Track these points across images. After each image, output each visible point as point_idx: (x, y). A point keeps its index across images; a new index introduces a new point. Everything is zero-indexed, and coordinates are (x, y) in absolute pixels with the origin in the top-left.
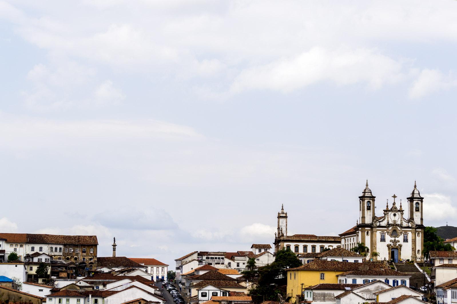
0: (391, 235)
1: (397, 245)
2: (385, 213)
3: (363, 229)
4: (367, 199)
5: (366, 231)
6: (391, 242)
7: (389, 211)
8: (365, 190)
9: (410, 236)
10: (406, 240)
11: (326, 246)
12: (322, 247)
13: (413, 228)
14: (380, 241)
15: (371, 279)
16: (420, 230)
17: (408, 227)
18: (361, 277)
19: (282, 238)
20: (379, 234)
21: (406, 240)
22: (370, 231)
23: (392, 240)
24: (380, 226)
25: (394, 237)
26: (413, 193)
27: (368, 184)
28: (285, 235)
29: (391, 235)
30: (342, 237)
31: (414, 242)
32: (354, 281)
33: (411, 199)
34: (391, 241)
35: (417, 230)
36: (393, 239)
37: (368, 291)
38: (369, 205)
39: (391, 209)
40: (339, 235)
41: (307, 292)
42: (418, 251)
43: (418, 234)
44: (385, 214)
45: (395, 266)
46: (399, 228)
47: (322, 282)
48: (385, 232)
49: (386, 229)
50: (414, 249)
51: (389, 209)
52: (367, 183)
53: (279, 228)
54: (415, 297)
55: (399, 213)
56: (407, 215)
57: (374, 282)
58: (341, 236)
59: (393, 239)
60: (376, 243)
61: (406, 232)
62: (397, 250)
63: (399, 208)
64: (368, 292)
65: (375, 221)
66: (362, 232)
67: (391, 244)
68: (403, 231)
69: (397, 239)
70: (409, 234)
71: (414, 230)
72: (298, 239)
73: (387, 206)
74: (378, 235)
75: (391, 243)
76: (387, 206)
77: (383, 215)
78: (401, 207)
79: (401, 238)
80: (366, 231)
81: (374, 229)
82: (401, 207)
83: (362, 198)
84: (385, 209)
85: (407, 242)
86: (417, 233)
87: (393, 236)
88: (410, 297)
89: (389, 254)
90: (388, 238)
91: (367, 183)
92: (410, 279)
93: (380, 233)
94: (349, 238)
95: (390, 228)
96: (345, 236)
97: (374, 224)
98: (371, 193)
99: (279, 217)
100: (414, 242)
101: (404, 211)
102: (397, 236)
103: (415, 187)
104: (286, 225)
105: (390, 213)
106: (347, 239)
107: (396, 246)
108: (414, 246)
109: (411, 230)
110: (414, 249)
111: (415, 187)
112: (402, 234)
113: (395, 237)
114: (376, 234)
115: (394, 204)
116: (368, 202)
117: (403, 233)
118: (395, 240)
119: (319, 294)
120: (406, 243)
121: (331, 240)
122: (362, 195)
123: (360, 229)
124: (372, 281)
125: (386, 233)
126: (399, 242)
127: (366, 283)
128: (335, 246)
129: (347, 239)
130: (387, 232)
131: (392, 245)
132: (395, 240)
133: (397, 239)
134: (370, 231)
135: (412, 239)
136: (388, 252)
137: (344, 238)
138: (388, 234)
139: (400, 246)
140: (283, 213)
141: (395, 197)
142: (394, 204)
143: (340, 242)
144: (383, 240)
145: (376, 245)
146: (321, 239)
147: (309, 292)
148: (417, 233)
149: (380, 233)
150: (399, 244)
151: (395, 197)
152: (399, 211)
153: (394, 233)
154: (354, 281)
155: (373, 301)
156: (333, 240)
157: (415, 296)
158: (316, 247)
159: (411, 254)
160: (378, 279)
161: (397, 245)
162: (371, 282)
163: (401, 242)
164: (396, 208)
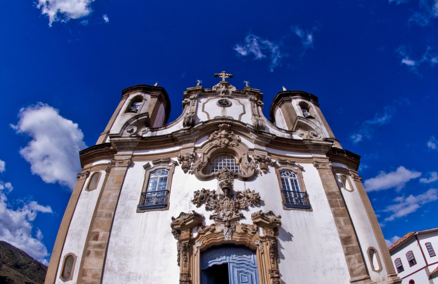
0: (204, 172)
1: (242, 221)
6: (204, 206)
14: (135, 209)
23: (204, 191)
25: (218, 176)
29: (206, 172)
36: (213, 185)
46: (248, 142)
59: (213, 185)
75: (201, 210)
87: (217, 173)
107: (239, 229)
110: (355, 244)
117: (274, 165)
120: (302, 214)
130: (182, 159)
131: (208, 222)
132: (228, 190)
133: (238, 186)
149: (147, 167)
159: (348, 273)
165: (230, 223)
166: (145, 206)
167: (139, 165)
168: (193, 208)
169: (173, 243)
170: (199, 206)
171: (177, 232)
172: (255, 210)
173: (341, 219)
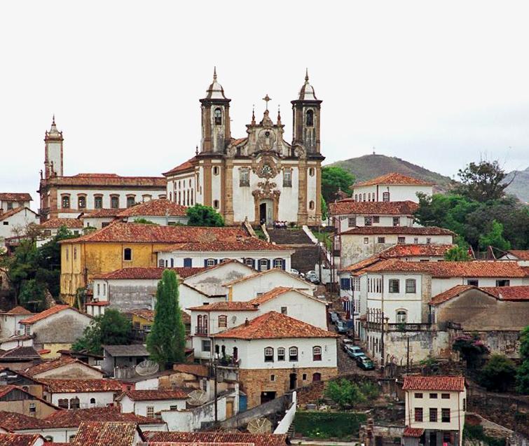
2: (249, 131)
3: (208, 161)
4: (215, 106)
5: (213, 166)
7: (258, 126)
8: (212, 86)
9: (295, 175)
10: (288, 184)
11: (139, 196)
12: (131, 199)
13: (302, 159)
15: (219, 259)
16: (315, 163)
17: (293, 158)
18: (201, 255)
19: (53, 181)
20: (238, 172)
21: (288, 184)
22: (220, 167)
24: (238, 157)
26: (303, 92)
27: (217, 73)
28: (59, 174)
30: (168, 178)
31: (303, 185)
32: (188, 262)
33: (298, 104)
34: (260, 185)
35: (309, 163)
36: (264, 180)
37: (213, 281)
38: (219, 116)
39: (261, 123)
40: (163, 174)
41: (99, 285)
42: (311, 203)
43: (311, 170)
44: (249, 133)
45: (266, 233)
47: (128, 265)
48: (250, 167)
49: (250, 161)
50: (303, 200)
51: (258, 123)
52: (215, 73)
53: (46, 162)
54: (299, 291)
55: (276, 131)
56: (288, 136)
57: (224, 263)
58: (167, 176)
59: (264, 180)
60: (232, 188)
61: (288, 166)
62: (272, 203)
63: (275, 123)
64: (213, 282)
65: (230, 146)
66: (205, 167)
67: (259, 191)
68: (282, 165)
69: (271, 181)
70: (293, 172)
71: (304, 162)
72: (84, 182)
73: (254, 118)
74: (236, 174)
75: (262, 190)
76: (254, 118)
77: (246, 135)
78: (279, 118)
79: (278, 180)
80: (213, 166)
81: (229, 163)
82: (279, 118)
83: (206, 103)
84: (250, 123)
85: (291, 186)
86: (309, 168)
88: (289, 290)
89: (256, 209)
90: (254, 179)
91: (215, 73)
92: (292, 257)
93: (239, 169)
94: (182, 181)
95: (259, 160)
96: (174, 175)
97: (228, 153)
98: (222, 91)
99: (48, 140)
100: (303, 185)
101: (284, 126)
102: (274, 175)
103: (307, 79)
104: (62, 155)
105: (258, 130)
106: (177, 182)
108: (303, 194)
109: (296, 162)
111: (307, 79)
112: (281, 171)
113: (268, 176)
114: (232, 173)
115: (266, 113)
116: (218, 109)
118: (267, 182)
119: (120, 288)
121: (148, 184)
122: (204, 96)
123: (201, 162)
124: (221, 261)
125: (250, 169)
126: (274, 185)
127: (208, 265)
128: (156, 195)
129: (177, 182)
130: (253, 168)
131: (262, 192)
132: (267, 182)
133: (271, 181)
134: (220, 167)
135: (299, 181)
136: (253, 206)
137: (173, 180)
138: (254, 172)
139: (278, 194)
140: (56, 131)
141: (267, 99)
142: (266, 113)
143: (164, 188)
144: (245, 183)
145: (232, 192)
146: (127, 184)
147: (102, 283)
148: (309, 168)
149: (239, 169)
150: (274, 191)
151: (267, 99)
152: (275, 126)
153: (267, 171)
154: (188, 262)
155: (222, 300)
156: (152, 184)
157: (298, 289)
158: (120, 198)
160: (232, 258)
161: (272, 192)
162: (218, 262)
163: (280, 187)
164: (270, 121)
165: (267, 193)
166: (242, 185)
167: (236, 167)
168: (257, 188)
169: (253, 197)
170: (259, 186)
171: (253, 194)
172: (275, 189)
173: (301, 191)
